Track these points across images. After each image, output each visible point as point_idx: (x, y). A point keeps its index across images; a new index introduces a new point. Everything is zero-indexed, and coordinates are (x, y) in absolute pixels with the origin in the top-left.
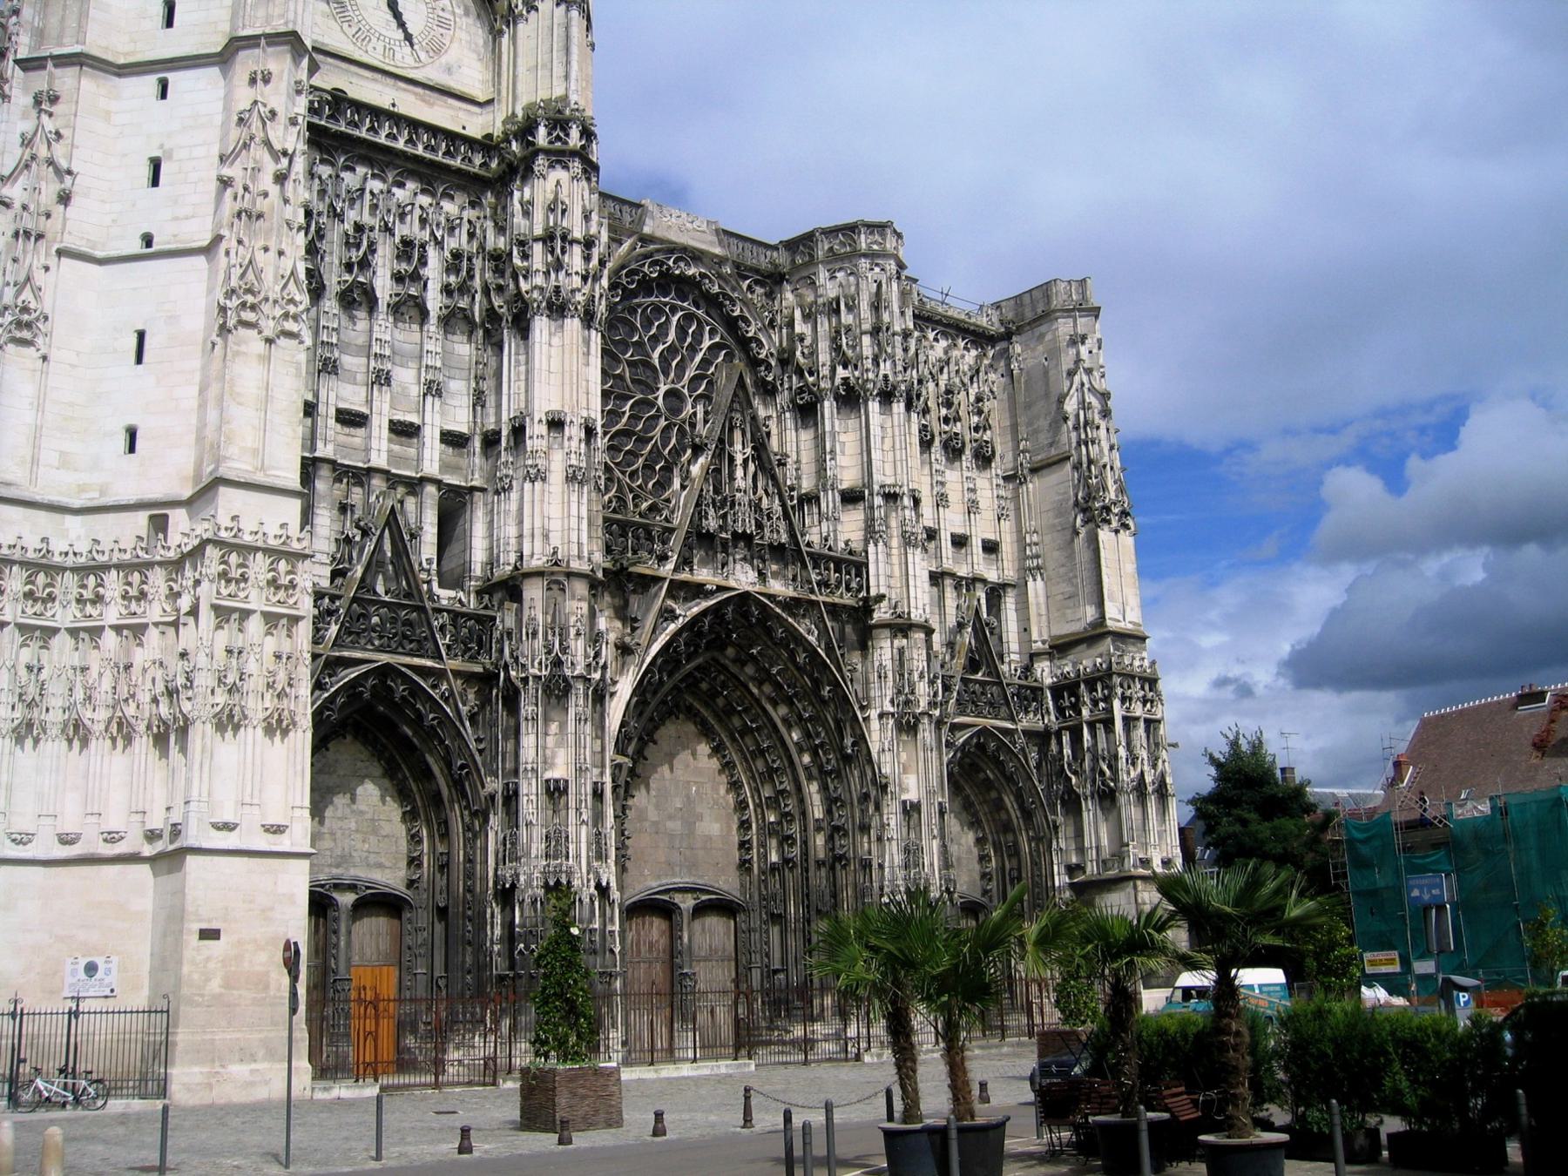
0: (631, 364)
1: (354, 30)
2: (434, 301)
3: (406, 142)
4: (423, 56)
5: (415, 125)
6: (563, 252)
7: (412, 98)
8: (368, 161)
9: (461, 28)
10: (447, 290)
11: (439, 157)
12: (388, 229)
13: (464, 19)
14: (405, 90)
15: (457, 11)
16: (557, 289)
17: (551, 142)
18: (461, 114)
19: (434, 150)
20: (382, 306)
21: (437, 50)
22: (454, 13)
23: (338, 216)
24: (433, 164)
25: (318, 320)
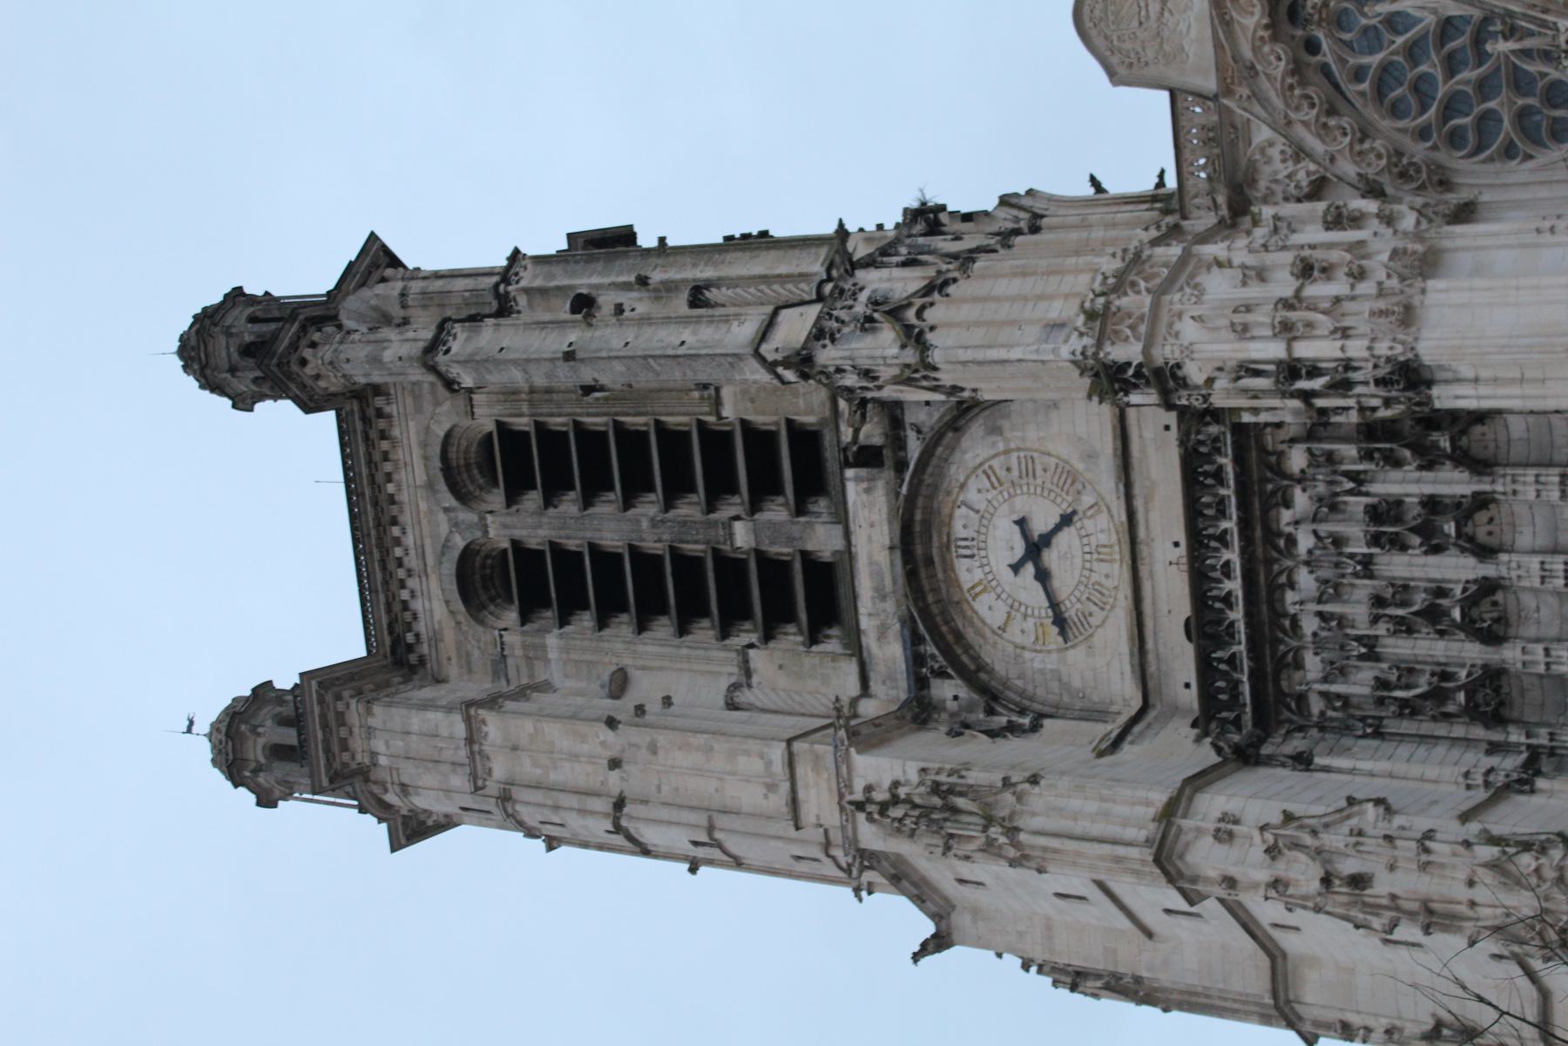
0: (1452, 65)
1: (1094, 609)
2: (1454, 483)
3: (1226, 545)
4: (1088, 499)
5: (1199, 541)
6: (1314, 372)
7: (1155, 517)
8: (1276, 591)
9: (1023, 439)
10: (1428, 466)
11: (1229, 492)
12: (1367, 562)
13: (1008, 434)
14: (1147, 528)
15: (1001, 446)
16: (1379, 382)
17: (1148, 383)
18: (1148, 434)
19: (1221, 504)
20: (1488, 570)
21: (1070, 478)
22: (1007, 452)
23: (1370, 643)
24: (1243, 505)
25: (1541, 676)
